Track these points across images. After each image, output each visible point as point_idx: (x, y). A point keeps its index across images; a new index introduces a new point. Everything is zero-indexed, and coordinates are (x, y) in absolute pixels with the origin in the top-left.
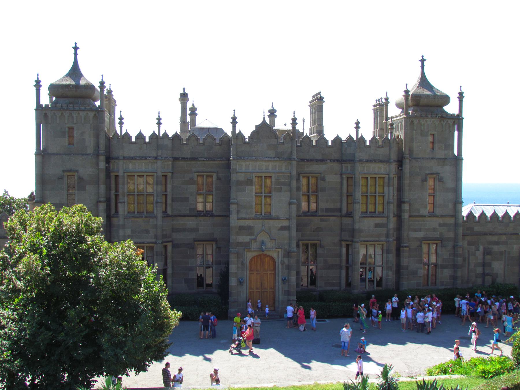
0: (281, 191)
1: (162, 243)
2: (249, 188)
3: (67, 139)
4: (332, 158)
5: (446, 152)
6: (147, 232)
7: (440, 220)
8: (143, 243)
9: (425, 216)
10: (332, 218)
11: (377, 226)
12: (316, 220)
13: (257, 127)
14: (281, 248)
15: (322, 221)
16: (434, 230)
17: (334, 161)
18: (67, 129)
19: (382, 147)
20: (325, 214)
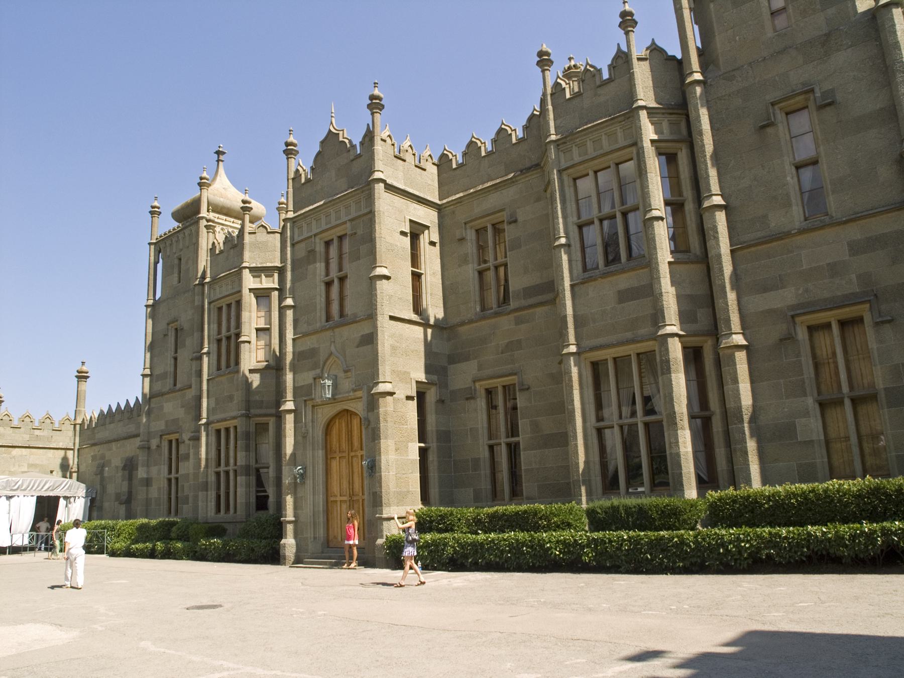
0: (358, 258)
1: (242, 415)
2: (311, 267)
3: (176, 275)
4: (528, 165)
5: (831, 11)
6: (231, 398)
7: (854, 232)
8: (225, 420)
9: (788, 235)
10: (539, 310)
11: (625, 296)
12: (505, 323)
13: (322, 143)
14: (360, 389)
15: (519, 321)
16: (835, 270)
17: (529, 169)
18: (176, 261)
19: (610, 80)
20: (524, 303)
